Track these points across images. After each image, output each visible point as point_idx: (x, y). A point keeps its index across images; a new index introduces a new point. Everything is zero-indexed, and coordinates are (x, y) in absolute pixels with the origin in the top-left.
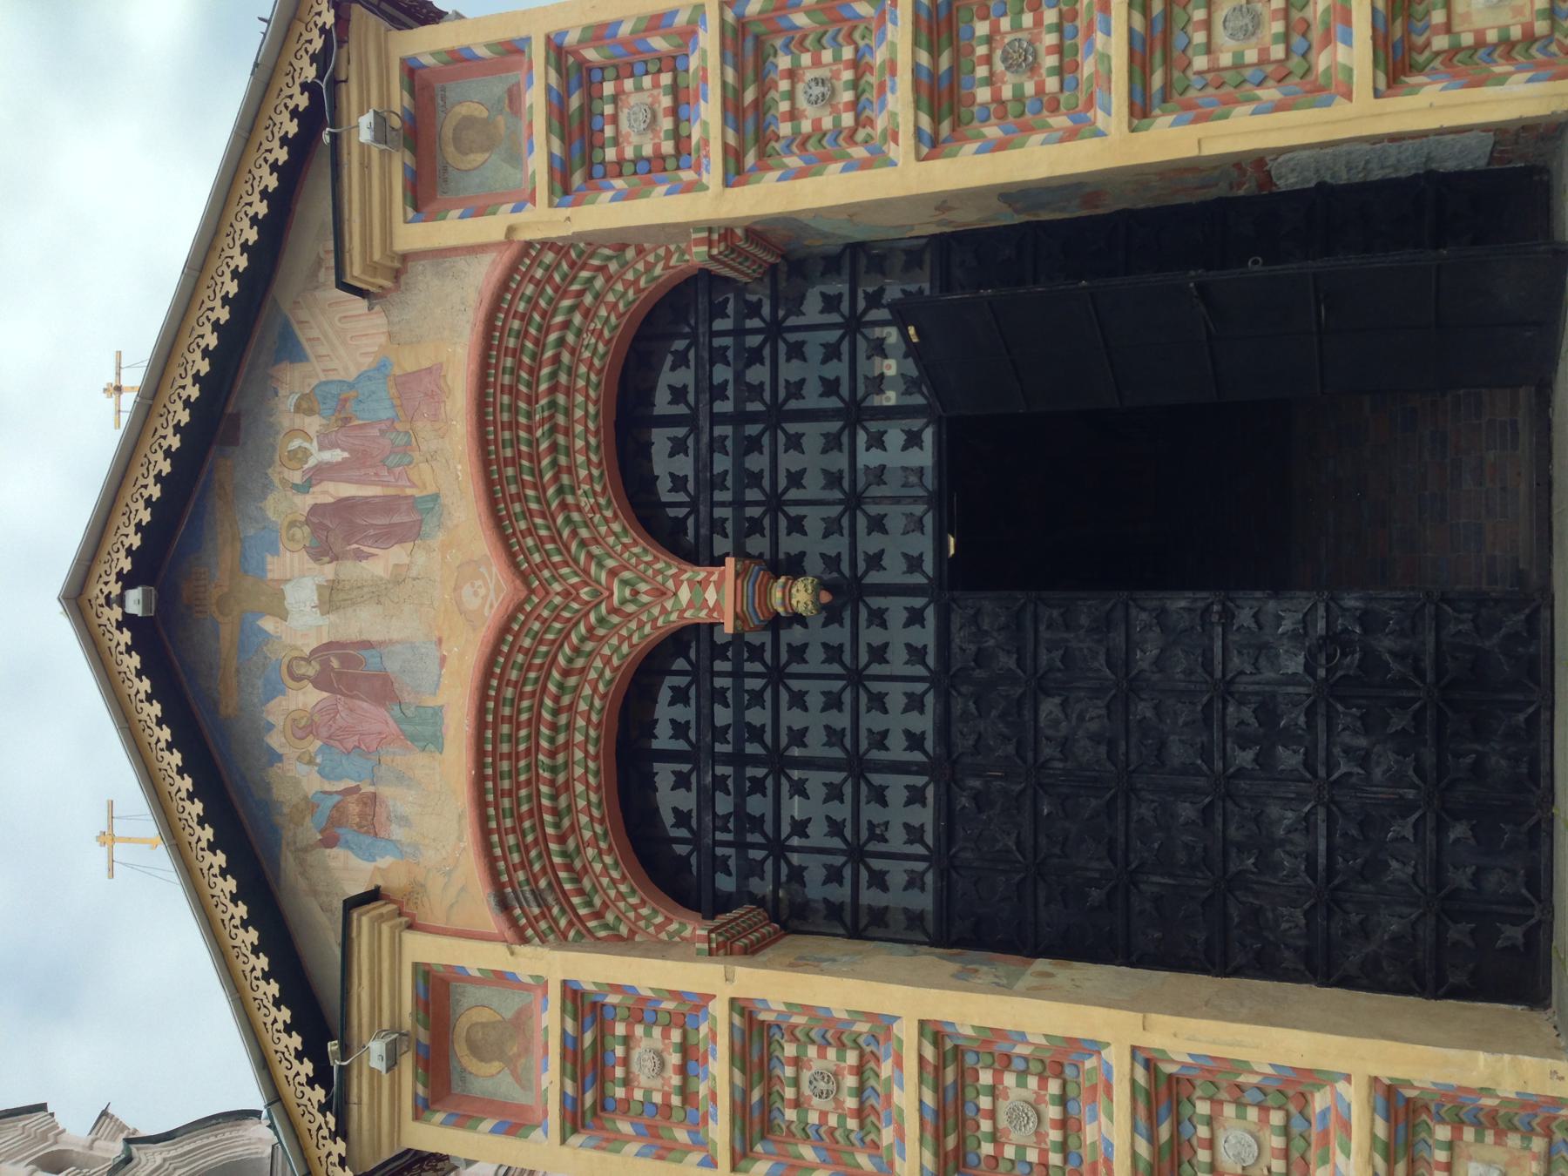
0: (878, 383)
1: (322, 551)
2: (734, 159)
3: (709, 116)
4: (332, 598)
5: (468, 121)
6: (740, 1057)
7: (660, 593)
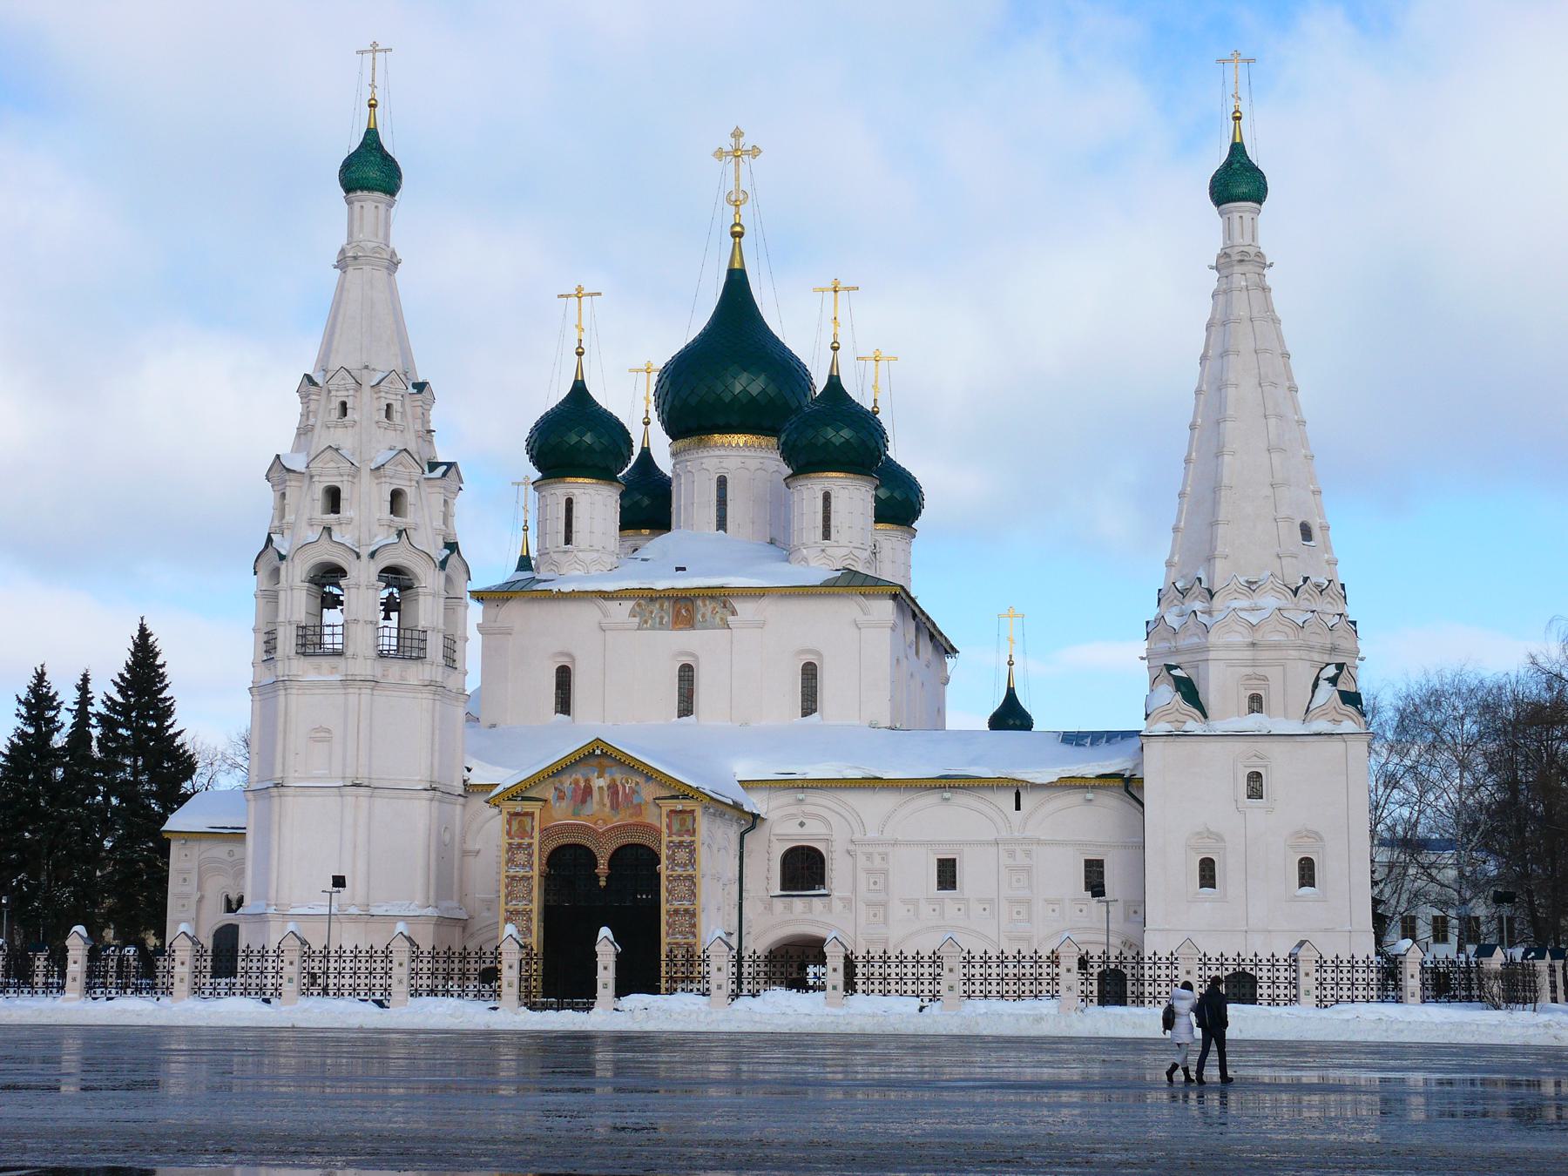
0: (642, 896)
1: (609, 787)
2: (671, 876)
3: (679, 871)
4: (599, 788)
5: (685, 821)
6: (523, 876)
7: (602, 857)
